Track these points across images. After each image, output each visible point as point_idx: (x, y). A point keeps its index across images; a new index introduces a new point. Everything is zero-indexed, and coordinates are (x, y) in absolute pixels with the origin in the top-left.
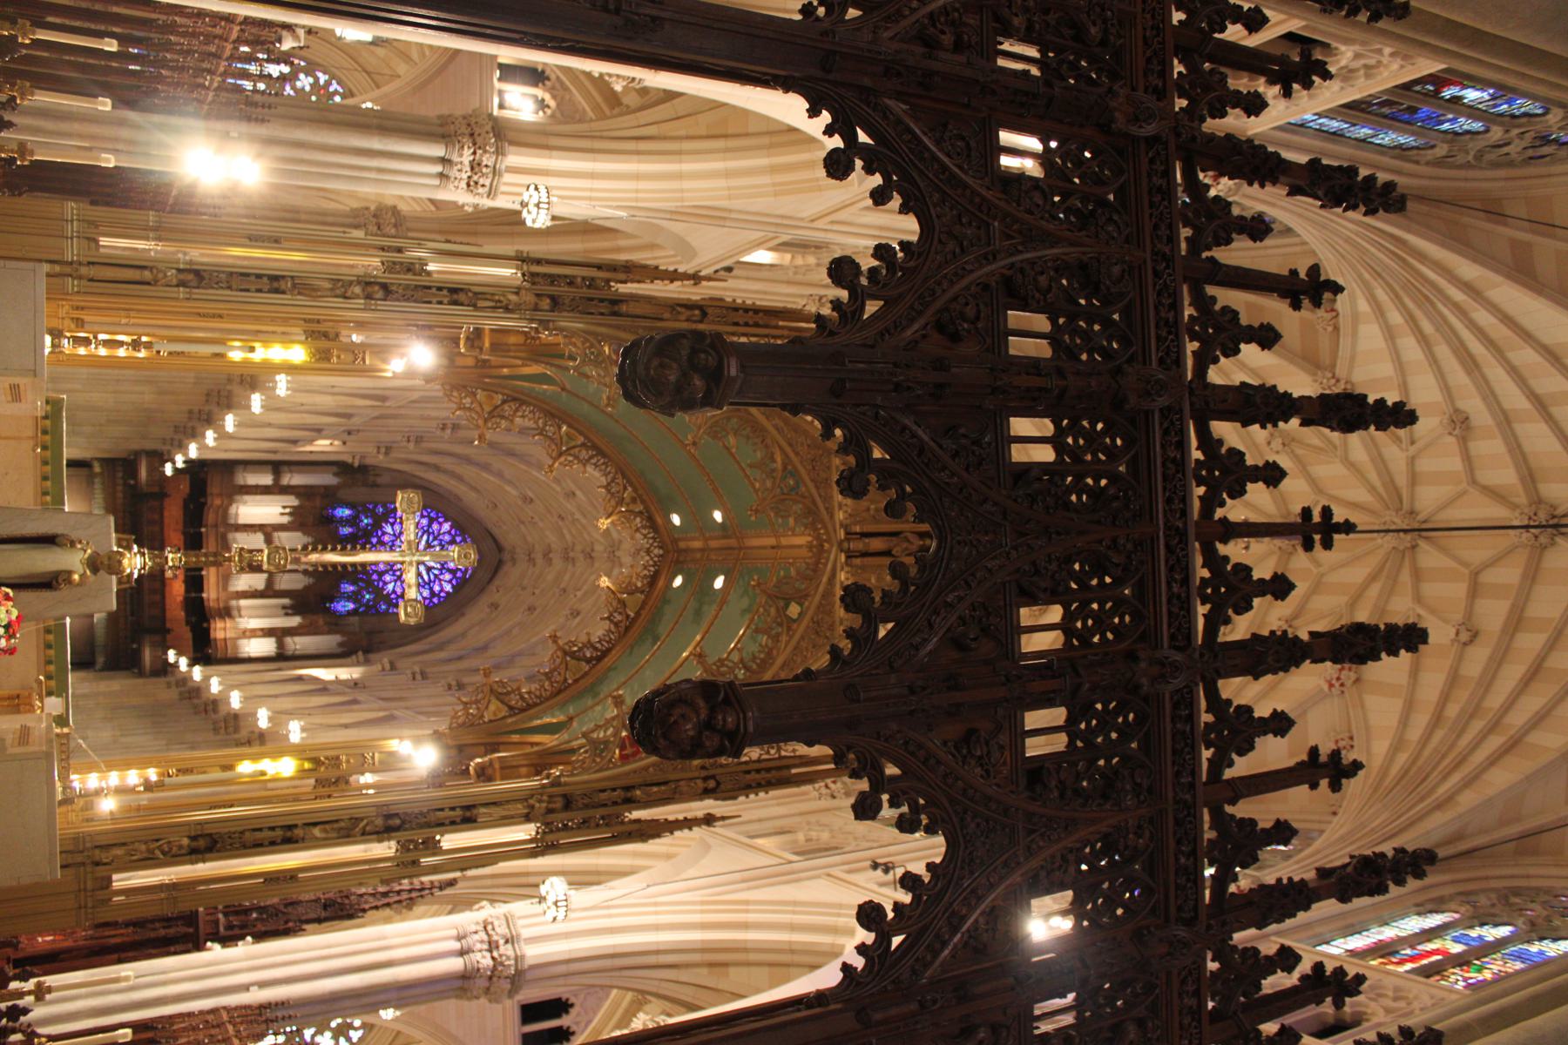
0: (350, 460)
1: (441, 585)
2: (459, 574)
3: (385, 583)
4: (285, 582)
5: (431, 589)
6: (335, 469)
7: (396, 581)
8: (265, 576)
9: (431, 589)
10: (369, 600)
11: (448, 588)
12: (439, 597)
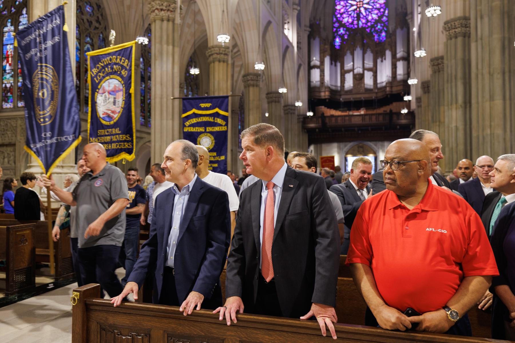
0: (308, 33)
3: (373, 19)
4: (369, 64)
6: (312, 40)
7: (371, 14)
8: (366, 72)
10: (381, 26)
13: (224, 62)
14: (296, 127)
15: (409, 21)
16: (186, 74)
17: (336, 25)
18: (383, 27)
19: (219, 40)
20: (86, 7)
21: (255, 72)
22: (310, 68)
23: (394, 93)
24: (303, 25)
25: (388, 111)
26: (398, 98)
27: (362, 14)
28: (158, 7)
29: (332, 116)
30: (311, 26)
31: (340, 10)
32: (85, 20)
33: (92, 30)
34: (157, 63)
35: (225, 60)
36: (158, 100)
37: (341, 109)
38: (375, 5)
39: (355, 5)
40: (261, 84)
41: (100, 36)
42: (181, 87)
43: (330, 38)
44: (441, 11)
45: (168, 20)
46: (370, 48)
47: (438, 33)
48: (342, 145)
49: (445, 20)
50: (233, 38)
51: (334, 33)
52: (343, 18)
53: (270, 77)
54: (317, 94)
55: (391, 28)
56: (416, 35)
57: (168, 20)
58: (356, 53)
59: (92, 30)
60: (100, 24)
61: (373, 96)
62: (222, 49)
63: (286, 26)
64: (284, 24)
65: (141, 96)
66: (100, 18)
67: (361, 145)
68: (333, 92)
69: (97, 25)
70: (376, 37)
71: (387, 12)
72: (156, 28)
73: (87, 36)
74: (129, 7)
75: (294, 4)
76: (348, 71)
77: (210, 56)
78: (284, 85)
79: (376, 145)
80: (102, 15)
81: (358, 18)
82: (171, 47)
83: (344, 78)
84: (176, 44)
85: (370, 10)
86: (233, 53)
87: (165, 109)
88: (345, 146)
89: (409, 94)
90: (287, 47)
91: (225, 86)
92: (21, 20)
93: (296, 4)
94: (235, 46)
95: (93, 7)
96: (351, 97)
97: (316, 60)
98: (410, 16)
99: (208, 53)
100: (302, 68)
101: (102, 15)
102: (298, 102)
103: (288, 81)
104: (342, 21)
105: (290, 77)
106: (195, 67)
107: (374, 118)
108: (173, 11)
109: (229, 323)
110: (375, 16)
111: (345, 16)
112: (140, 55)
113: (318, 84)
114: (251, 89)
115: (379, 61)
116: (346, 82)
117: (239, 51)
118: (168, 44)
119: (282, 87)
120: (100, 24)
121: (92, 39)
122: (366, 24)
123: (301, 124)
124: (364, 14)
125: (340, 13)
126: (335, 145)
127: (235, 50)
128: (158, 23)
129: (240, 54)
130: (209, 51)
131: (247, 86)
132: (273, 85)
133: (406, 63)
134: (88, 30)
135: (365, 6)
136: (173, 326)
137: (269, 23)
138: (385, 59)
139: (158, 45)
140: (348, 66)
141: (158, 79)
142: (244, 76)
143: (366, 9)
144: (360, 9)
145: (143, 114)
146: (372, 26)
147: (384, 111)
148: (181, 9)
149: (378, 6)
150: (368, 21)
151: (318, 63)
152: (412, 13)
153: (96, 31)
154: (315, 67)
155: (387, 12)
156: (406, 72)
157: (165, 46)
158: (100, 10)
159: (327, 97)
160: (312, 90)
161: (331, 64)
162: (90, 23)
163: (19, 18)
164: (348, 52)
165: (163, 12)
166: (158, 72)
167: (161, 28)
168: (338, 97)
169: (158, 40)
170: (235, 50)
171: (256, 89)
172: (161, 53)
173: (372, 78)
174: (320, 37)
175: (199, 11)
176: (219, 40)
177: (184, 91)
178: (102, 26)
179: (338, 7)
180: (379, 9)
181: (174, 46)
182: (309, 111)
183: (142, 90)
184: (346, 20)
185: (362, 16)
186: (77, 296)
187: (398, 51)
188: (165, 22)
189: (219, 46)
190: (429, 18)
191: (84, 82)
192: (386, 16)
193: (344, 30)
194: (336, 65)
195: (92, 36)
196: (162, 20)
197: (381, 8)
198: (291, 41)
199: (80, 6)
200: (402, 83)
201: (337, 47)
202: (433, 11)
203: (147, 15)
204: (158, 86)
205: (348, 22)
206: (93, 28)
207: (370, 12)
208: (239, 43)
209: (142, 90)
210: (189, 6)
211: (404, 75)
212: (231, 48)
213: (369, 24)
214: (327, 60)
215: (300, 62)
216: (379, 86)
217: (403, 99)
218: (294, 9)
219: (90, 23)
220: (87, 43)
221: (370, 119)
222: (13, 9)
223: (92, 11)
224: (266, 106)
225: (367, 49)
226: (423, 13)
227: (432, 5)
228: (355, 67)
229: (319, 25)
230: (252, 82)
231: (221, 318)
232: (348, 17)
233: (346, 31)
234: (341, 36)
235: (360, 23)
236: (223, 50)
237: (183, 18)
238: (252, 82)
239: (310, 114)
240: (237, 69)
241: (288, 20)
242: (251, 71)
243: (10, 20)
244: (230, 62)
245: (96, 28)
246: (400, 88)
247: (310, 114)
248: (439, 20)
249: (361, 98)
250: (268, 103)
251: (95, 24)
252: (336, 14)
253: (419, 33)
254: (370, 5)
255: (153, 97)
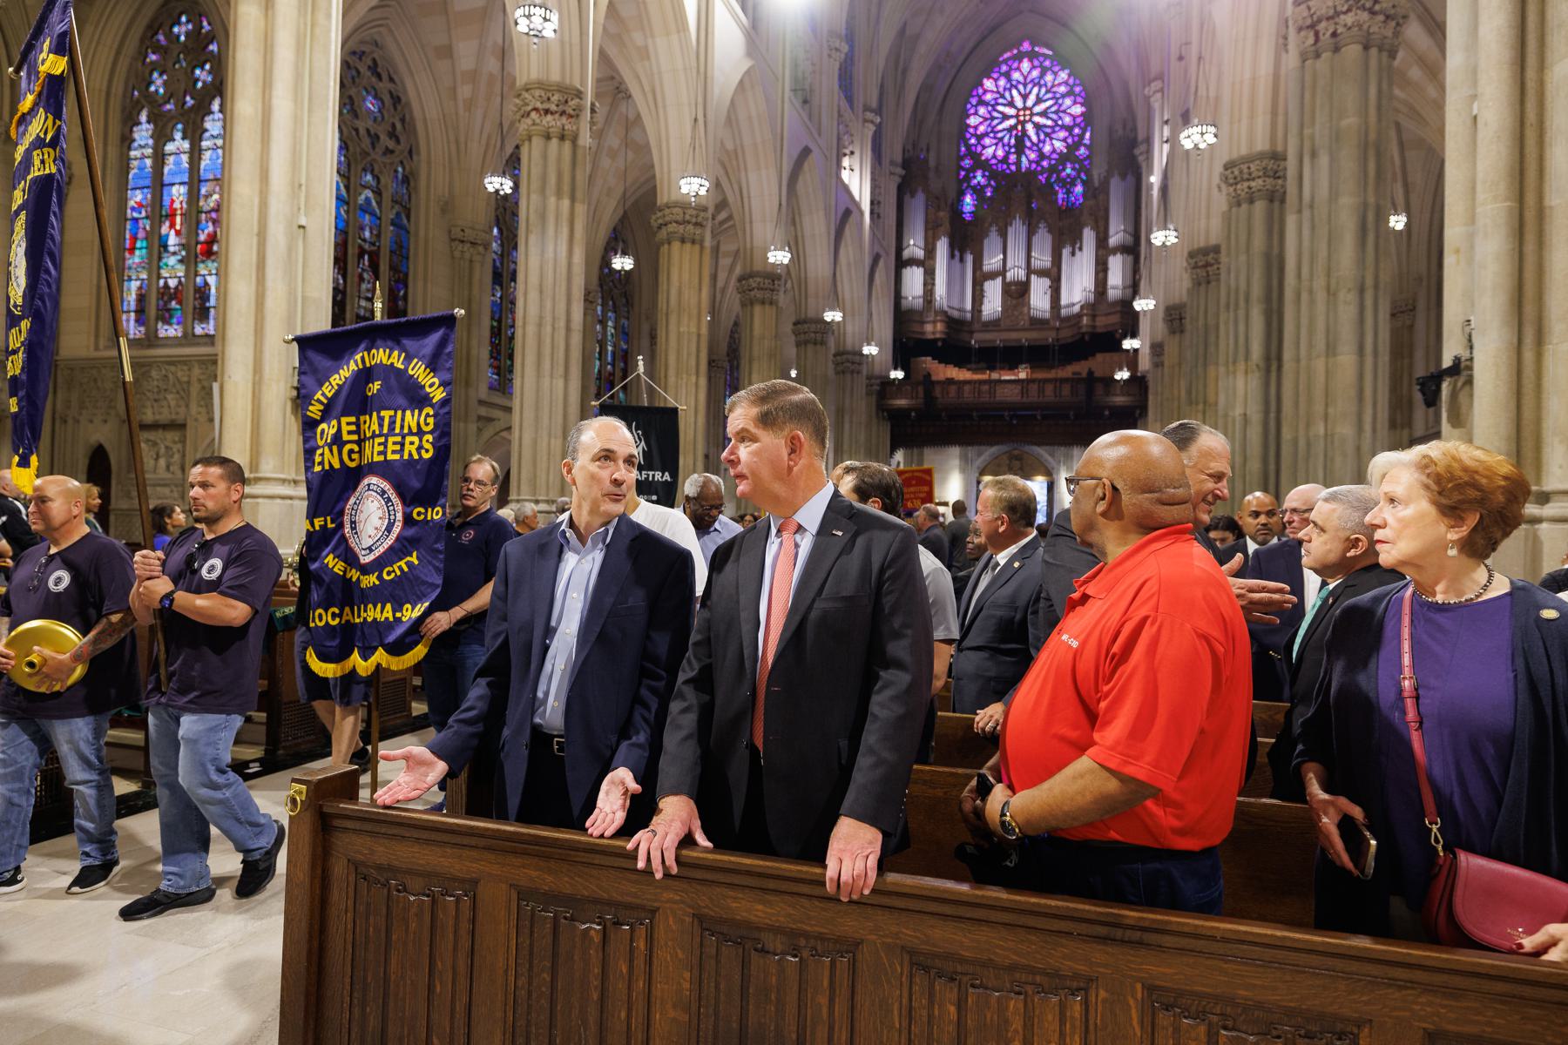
0: (898, 180)
1: (1060, 84)
2: (1047, 63)
3: (1054, 151)
4: (1042, 259)
5: (1063, 96)
6: (907, 198)
7: (1051, 139)
8: (1033, 278)
9: (1063, 96)
10: (1073, 169)
11: (1063, 75)
12: (1075, 85)
13: (693, 242)
14: (861, 405)
15: (1141, 158)
16: (601, 268)
17: (967, 163)
18: (1079, 174)
19: (684, 190)
20: (364, 101)
21: (769, 269)
22: (901, 263)
23: (1099, 330)
24: (886, 161)
25: (1084, 375)
26: (1108, 342)
27: (1031, 140)
28: (539, 105)
29: (950, 381)
30: (906, 164)
31: (976, 128)
32: (362, 132)
33: (377, 155)
34: (533, 238)
35: (697, 237)
36: (531, 329)
37: (973, 366)
38: (1060, 118)
39: (1012, 117)
40: (782, 299)
41: (396, 171)
42: (588, 300)
43: (952, 194)
44: (1216, 136)
45: (562, 138)
46: (1046, 221)
47: (1209, 189)
48: (971, 451)
49: (1226, 158)
50: (717, 185)
51: (960, 182)
52: (984, 147)
53: (803, 283)
54: (916, 328)
55: (1097, 173)
56: (1155, 192)
57: (562, 138)
58: (1011, 231)
59: (377, 155)
60: (398, 141)
61: (1050, 337)
62: (690, 212)
63: (846, 162)
64: (840, 156)
65: (492, 319)
66: (399, 126)
67: (1016, 452)
68: (955, 325)
69: (391, 144)
70: (1060, 196)
71: (1088, 135)
72: (532, 155)
73: (364, 170)
74: (470, 105)
75: (867, 108)
76: (992, 276)
77: (659, 228)
78: (836, 304)
79: (1052, 455)
80: (403, 120)
81: (1020, 148)
82: (566, 203)
83: (982, 290)
84: (579, 194)
85: (1048, 130)
86: (716, 222)
87: (547, 351)
88: (979, 455)
89: (1134, 335)
90: (847, 213)
91: (694, 301)
92: (208, 125)
93: (872, 111)
94: (722, 205)
95: (383, 103)
96: (997, 338)
97: (914, 246)
98: (1142, 148)
99: (655, 220)
100: (881, 263)
101: (403, 120)
102: (869, 344)
103: (847, 296)
104: (981, 154)
105: (853, 285)
106: (624, 253)
107: (1049, 389)
108: (575, 116)
109: (659, 876)
110: (1058, 145)
111: (987, 141)
112: (493, 218)
113: (919, 303)
114: (757, 309)
115: (1066, 252)
116: (986, 301)
117: (730, 218)
118: (559, 194)
119: (832, 309)
120: (398, 141)
121: (377, 178)
122: (1037, 162)
123: (874, 398)
124: (1034, 138)
125: (975, 135)
126: (955, 452)
127: (723, 215)
128: (537, 142)
129: (734, 226)
130: (659, 214)
131: (747, 303)
132: (811, 301)
133: (1130, 259)
134: (368, 154)
135: (1037, 119)
136: (534, 874)
137: (806, 152)
138: (1081, 249)
139: (534, 197)
140: (992, 262)
141: (534, 280)
142: (740, 280)
143: (1038, 127)
144: (1023, 127)
145: (496, 363)
146: (1053, 170)
147: (1074, 373)
148: (593, 111)
149: (1067, 120)
150: (1042, 156)
151: (920, 253)
152: (1148, 141)
153: (387, 160)
154: (913, 262)
155: (1088, 135)
156: (1129, 282)
157: (552, 200)
158: (399, 108)
159: (938, 336)
160: (903, 317)
161: (952, 256)
162: (375, 139)
163: (202, 120)
164: (994, 229)
165: (549, 117)
166: (534, 262)
167: (545, 157)
168: (965, 336)
169: (535, 185)
170: (723, 215)
171: (770, 311)
172: (543, 217)
173: (1049, 292)
174: (927, 191)
175: (638, 117)
176: (684, 190)
177: (595, 310)
178: (404, 146)
179: (973, 121)
180: (1069, 129)
181: (573, 199)
182: (896, 369)
183: (494, 303)
184: (989, 152)
185: (1028, 144)
186: (300, 793)
187: (1112, 230)
188: (555, 141)
189: (684, 205)
190: (1187, 151)
191: (356, 279)
192: (1085, 145)
193: (983, 176)
194: (962, 260)
195: (376, 172)
196: (548, 137)
197: (1075, 125)
198: (857, 198)
199: (350, 97)
200: (1119, 308)
201: (967, 217)
202: (1196, 137)
203: (512, 124)
204: (533, 295)
205: (994, 156)
206: (380, 149)
207: (1047, 135)
208: (731, 199)
209: (494, 303)
210: (613, 106)
211: (1124, 288)
212: (711, 210)
213: (1045, 163)
214: (942, 247)
215: (877, 249)
216: (1063, 312)
217: (1121, 344)
218: (865, 121)
219: (375, 139)
220: (365, 187)
221: (1041, 391)
222: (188, 98)
223: (380, 111)
224: (791, 351)
225: (1038, 222)
226: (1173, 141)
227: (1196, 121)
228: (1009, 264)
229: (926, 160)
230: (759, 294)
231: (641, 864)
232: (996, 144)
233: (989, 178)
234: (978, 191)
235: (1024, 159)
236: (693, 214)
237: (599, 135)
238: (759, 294)
239: (898, 374)
240: (725, 262)
241: (851, 148)
242: (758, 267)
243: (180, 126)
244: (708, 242)
245: (388, 151)
246: (1115, 319)
247: (898, 374)
248: (1212, 159)
249: (1020, 340)
250: (798, 344)
251: (386, 141)
252: (968, 136)
253: (1164, 189)
254: (1048, 118)
255: (519, 323)
